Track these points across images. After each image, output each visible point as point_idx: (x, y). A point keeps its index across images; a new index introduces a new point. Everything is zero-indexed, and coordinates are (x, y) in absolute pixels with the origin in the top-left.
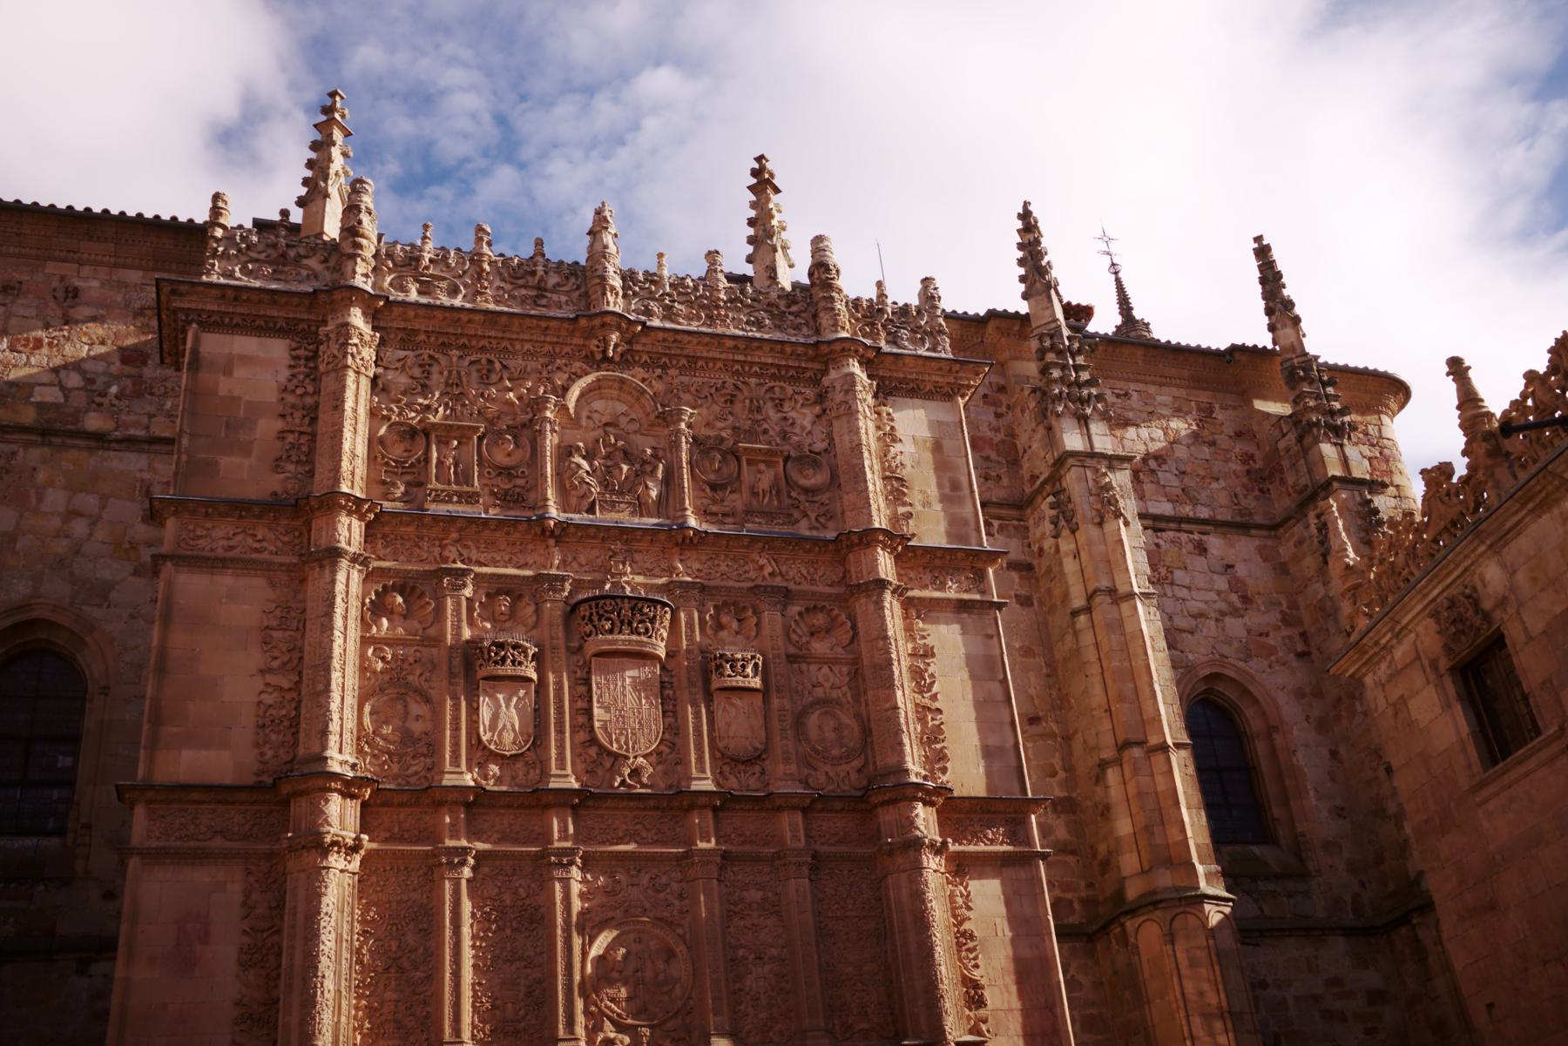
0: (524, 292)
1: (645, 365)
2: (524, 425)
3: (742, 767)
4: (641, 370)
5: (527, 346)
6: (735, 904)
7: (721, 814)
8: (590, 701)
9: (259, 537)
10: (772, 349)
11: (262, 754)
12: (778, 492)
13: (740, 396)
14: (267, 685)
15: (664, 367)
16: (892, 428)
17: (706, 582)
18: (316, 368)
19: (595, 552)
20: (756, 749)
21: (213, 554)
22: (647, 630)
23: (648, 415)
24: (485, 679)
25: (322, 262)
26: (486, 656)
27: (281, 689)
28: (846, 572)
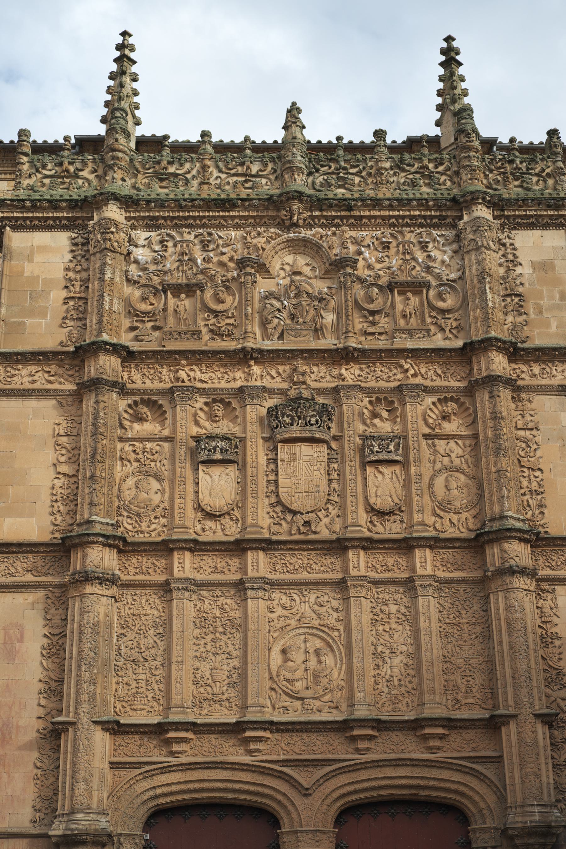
0: (235, 178)
1: (322, 226)
2: (234, 278)
3: (387, 517)
4: (320, 230)
5: (237, 221)
7: (369, 552)
8: (277, 475)
9: (52, 373)
10: (419, 205)
11: (56, 519)
12: (422, 313)
13: (394, 243)
14: (59, 473)
15: (337, 226)
16: (514, 255)
17: (363, 385)
18: (88, 251)
19: (281, 369)
21: (21, 387)
23: (324, 263)
24: (203, 462)
25: (93, 172)
26: (203, 447)
27: (68, 475)
28: (471, 370)
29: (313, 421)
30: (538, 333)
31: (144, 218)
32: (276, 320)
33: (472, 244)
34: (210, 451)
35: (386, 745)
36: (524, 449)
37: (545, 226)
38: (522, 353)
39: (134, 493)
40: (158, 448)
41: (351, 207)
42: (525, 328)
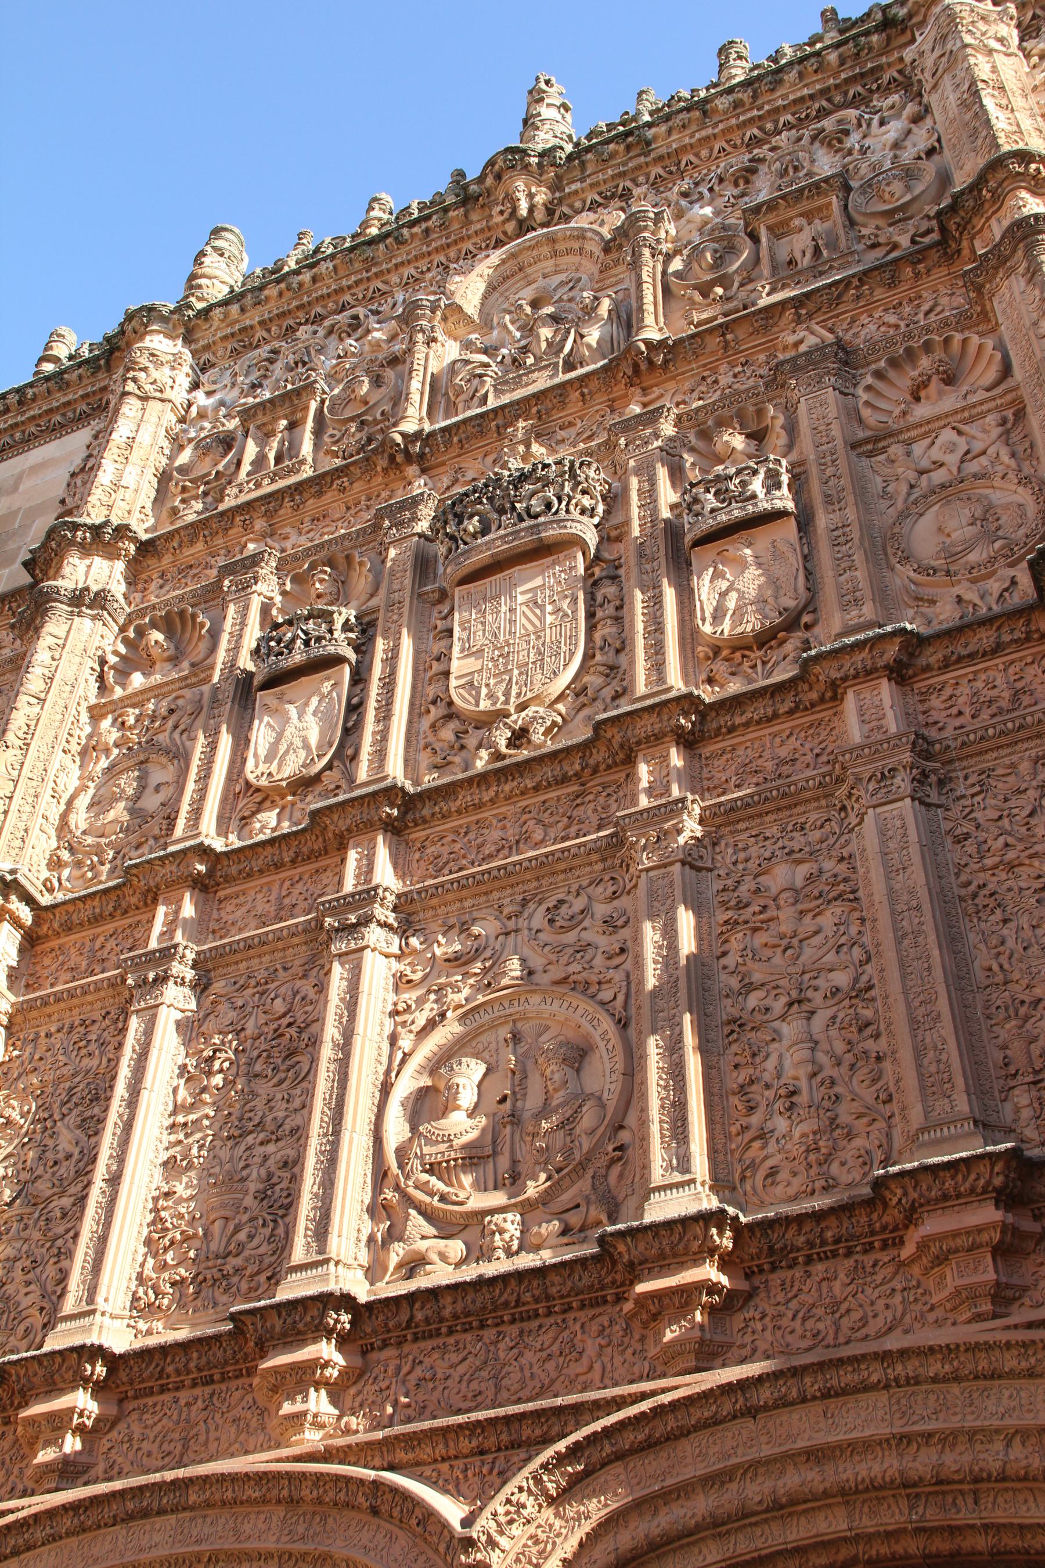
5: (409, 271)
6: (742, 906)
7: (707, 750)
22: (549, 506)
31: (225, 338)
35: (785, 1322)
40: (180, 702)
41: (648, 143)
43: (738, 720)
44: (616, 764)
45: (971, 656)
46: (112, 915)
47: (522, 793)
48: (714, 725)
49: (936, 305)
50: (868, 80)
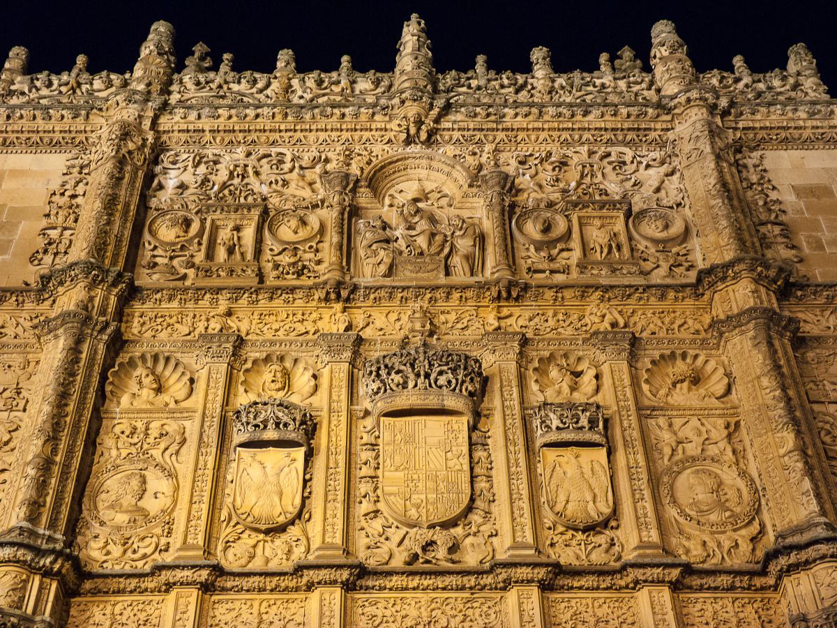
5: (322, 135)
16: (762, 177)
20: (600, 513)
22: (449, 382)
24: (243, 445)
26: (244, 420)
29: (442, 380)
30: (820, 273)
32: (382, 253)
33: (694, 155)
34: (256, 426)
36: (829, 433)
37: (806, 144)
38: (799, 293)
39: (114, 498)
42: (798, 265)
43: (576, 584)
44: (496, 588)
45: (716, 588)
46: (131, 592)
47: (434, 590)
48: (561, 583)
49: (685, 323)
50: (641, 133)
